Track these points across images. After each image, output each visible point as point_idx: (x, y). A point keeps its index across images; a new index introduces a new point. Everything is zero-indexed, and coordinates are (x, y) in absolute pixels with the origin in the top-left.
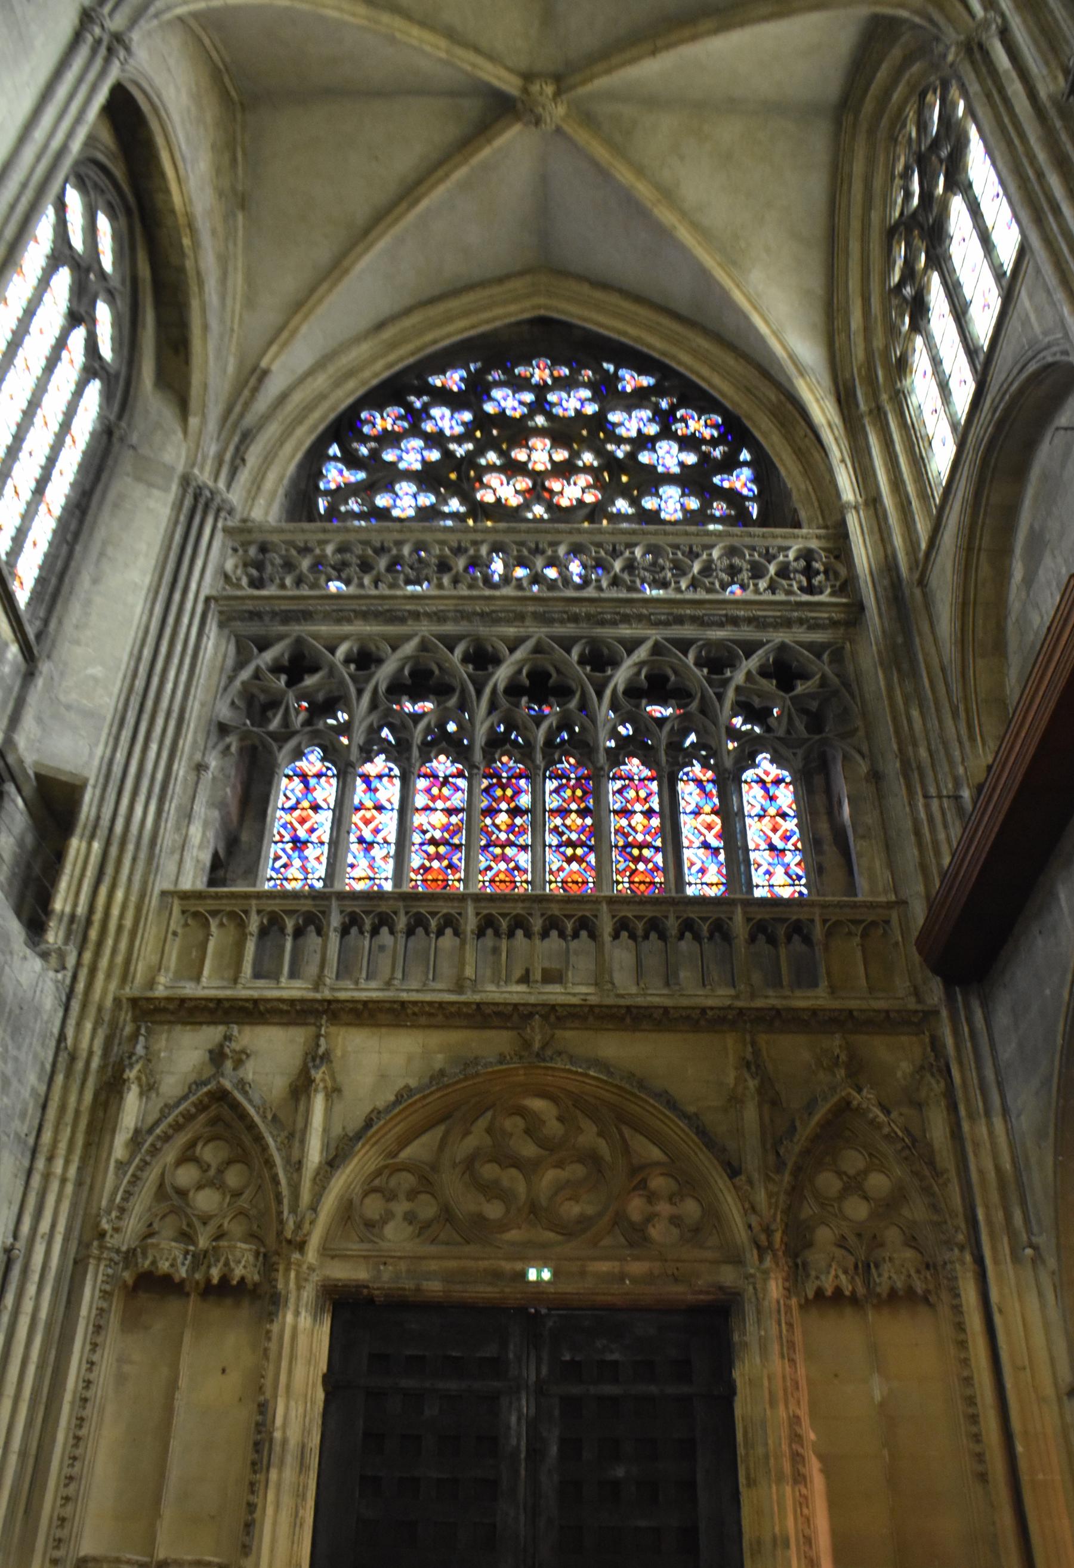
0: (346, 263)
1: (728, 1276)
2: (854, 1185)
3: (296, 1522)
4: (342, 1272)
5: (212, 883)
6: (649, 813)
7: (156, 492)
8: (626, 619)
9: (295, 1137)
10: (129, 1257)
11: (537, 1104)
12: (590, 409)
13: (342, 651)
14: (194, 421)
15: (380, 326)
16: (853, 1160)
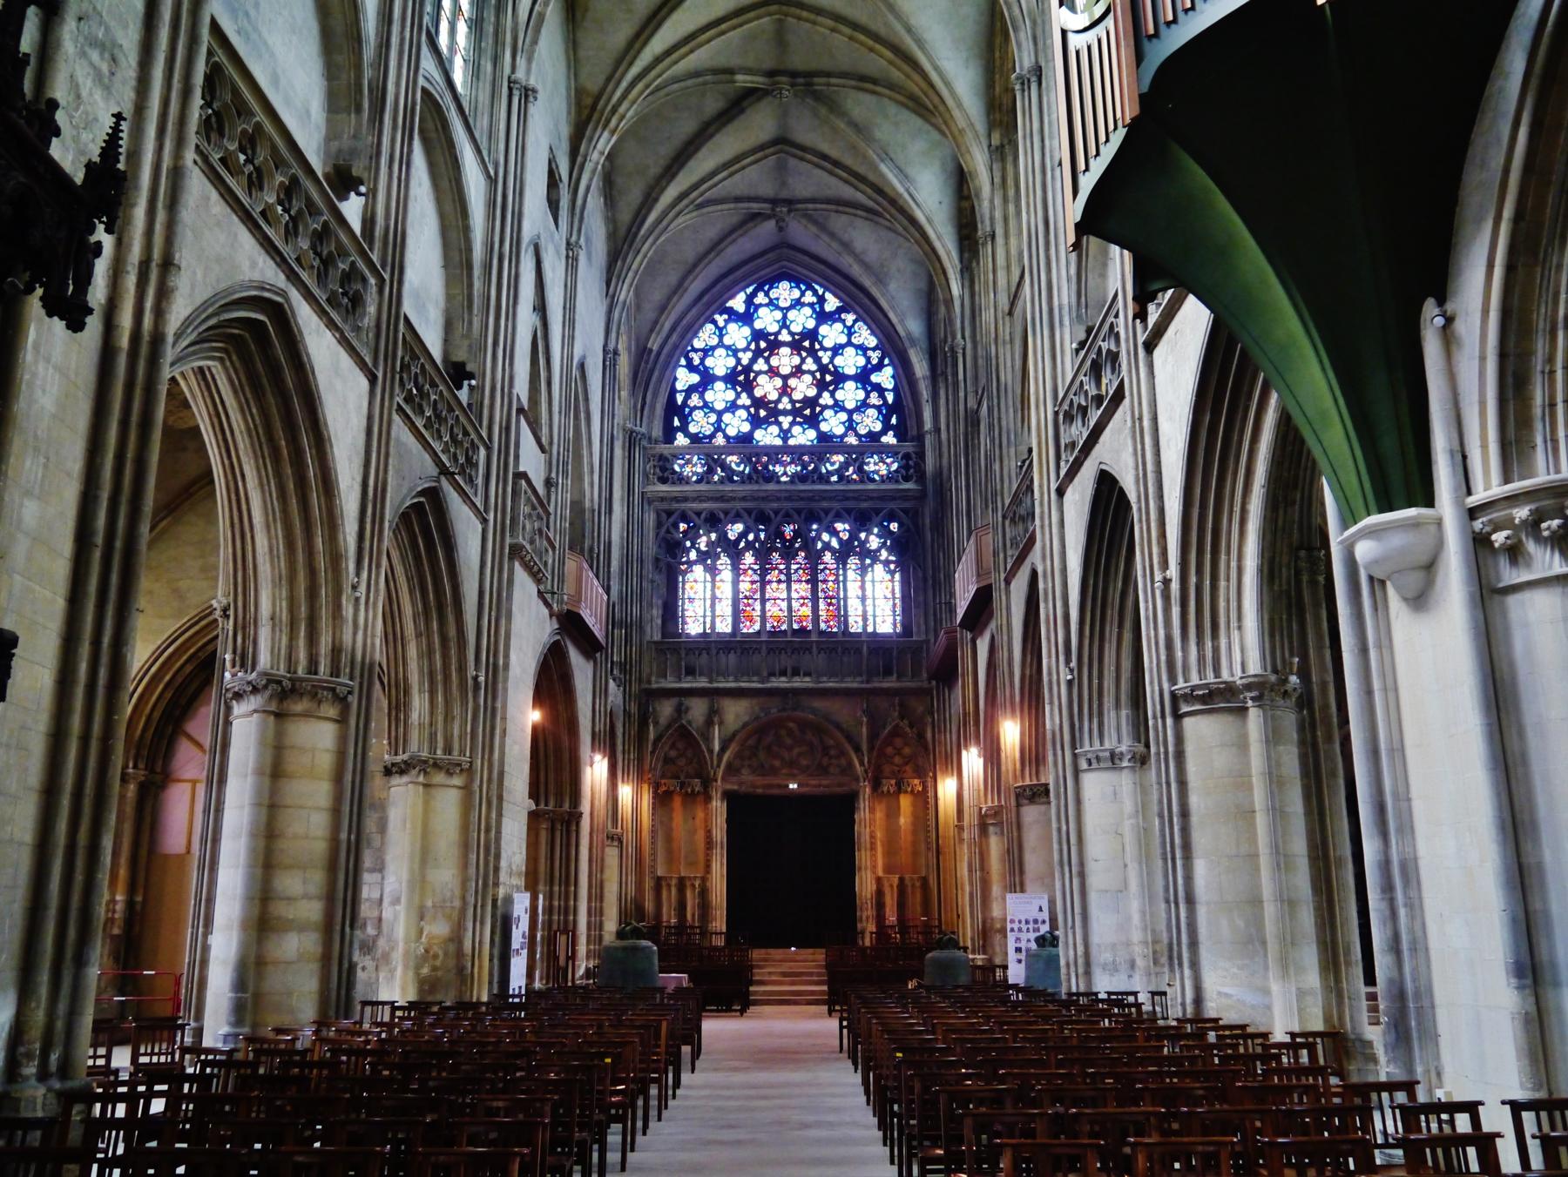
0: (686, 285)
1: (854, 787)
2: (899, 752)
3: (722, 864)
4: (729, 787)
5: (664, 636)
8: (824, 499)
9: (708, 739)
11: (791, 725)
12: (811, 324)
13: (703, 516)
16: (898, 742)
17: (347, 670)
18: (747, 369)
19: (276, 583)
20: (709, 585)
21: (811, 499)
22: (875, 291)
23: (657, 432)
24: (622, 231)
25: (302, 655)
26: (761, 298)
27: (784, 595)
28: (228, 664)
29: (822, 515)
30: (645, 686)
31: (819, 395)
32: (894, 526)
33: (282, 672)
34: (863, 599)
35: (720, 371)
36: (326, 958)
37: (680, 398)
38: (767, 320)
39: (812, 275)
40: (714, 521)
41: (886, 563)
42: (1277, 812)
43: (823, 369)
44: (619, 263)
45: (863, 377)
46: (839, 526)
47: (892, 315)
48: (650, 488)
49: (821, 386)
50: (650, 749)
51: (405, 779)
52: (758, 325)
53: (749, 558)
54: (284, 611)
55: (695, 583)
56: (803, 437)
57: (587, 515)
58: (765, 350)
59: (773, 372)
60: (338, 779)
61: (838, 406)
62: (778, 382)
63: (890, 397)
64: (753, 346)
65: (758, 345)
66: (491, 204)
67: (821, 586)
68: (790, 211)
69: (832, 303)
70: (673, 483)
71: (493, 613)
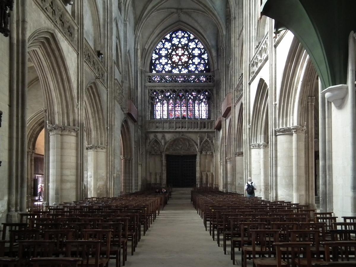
5: (151, 119)
6: (192, 106)
8: (190, 87)
12: (187, 42)
13: (160, 91)
17: (77, 125)
18: (171, 54)
19: (58, 104)
20: (161, 107)
21: (187, 86)
22: (203, 34)
23: (148, 69)
24: (138, 17)
25: (66, 121)
26: (174, 35)
27: (180, 110)
28: (48, 123)
31: (189, 61)
32: (207, 93)
33: (61, 124)
34: (199, 111)
35: (163, 54)
36: (77, 188)
37: (153, 61)
38: (175, 41)
41: (205, 102)
42: (298, 157)
43: (190, 54)
44: (137, 25)
45: (200, 56)
46: (193, 93)
47: (207, 40)
49: (189, 58)
51: (92, 150)
52: (173, 42)
53: (171, 101)
54: (61, 111)
55: (158, 107)
56: (184, 71)
59: (177, 55)
60: (77, 150)
61: (193, 64)
62: (178, 57)
63: (206, 61)
64: (172, 48)
65: (173, 48)
66: (104, 8)
67: (189, 108)
68: (181, 12)
69: (192, 37)
71: (111, 113)
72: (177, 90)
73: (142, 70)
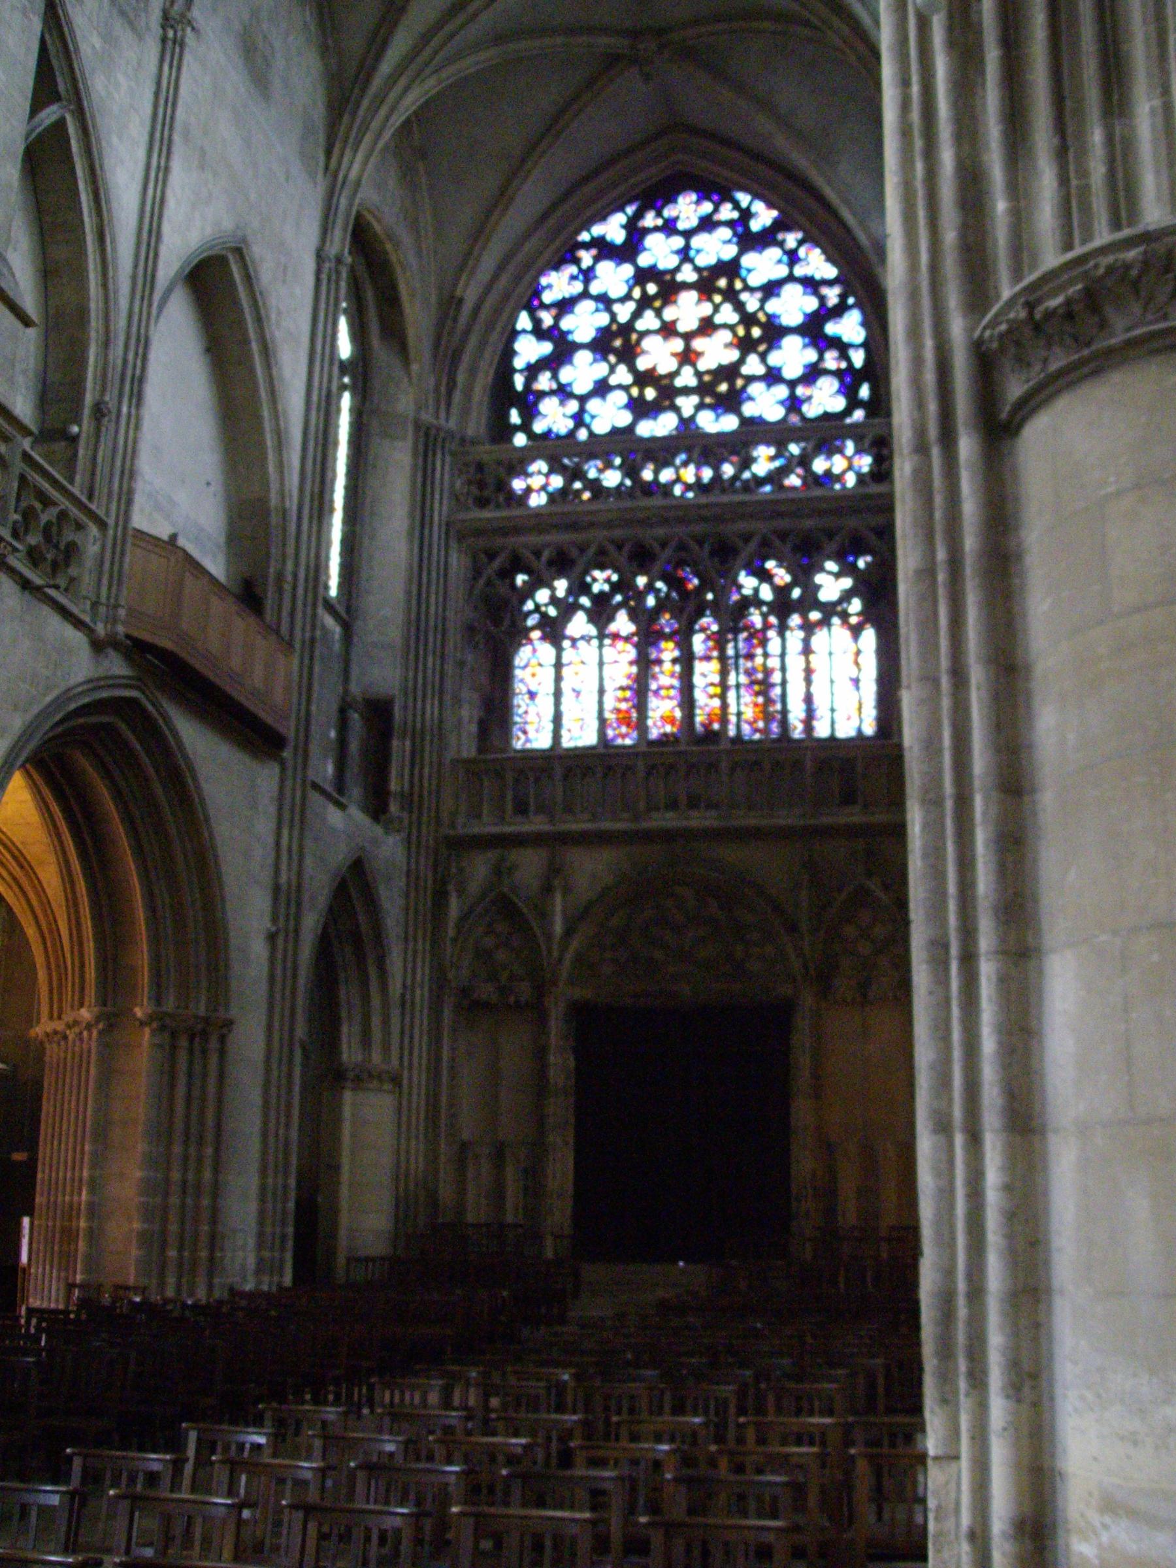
4: (578, 993)
5: (480, 750)
7: (400, 444)
8: (742, 517)
10: (464, 992)
12: (729, 252)
14: (415, 367)
15: (544, 217)
21: (718, 519)
22: (819, 181)
29: (740, 544)
30: (446, 831)
37: (519, 382)
39: (726, 173)
40: (562, 564)
43: (748, 320)
44: (346, 118)
48: (461, 516)
49: (746, 345)
50: (451, 932)
52: (644, 260)
57: (274, 519)
58: (655, 297)
61: (773, 377)
69: (763, 216)
70: (498, 506)
72: (655, 545)
73: (433, 432)
